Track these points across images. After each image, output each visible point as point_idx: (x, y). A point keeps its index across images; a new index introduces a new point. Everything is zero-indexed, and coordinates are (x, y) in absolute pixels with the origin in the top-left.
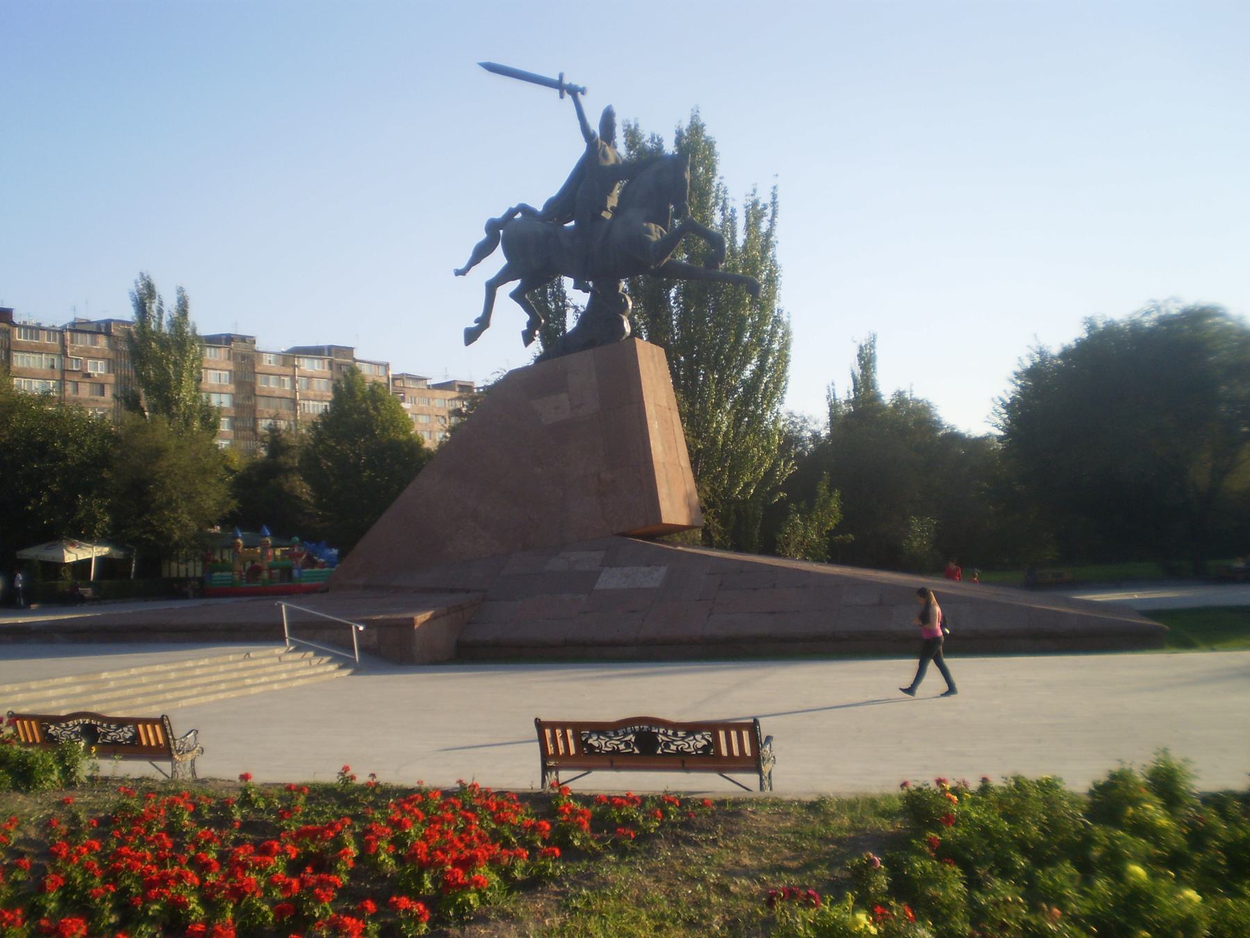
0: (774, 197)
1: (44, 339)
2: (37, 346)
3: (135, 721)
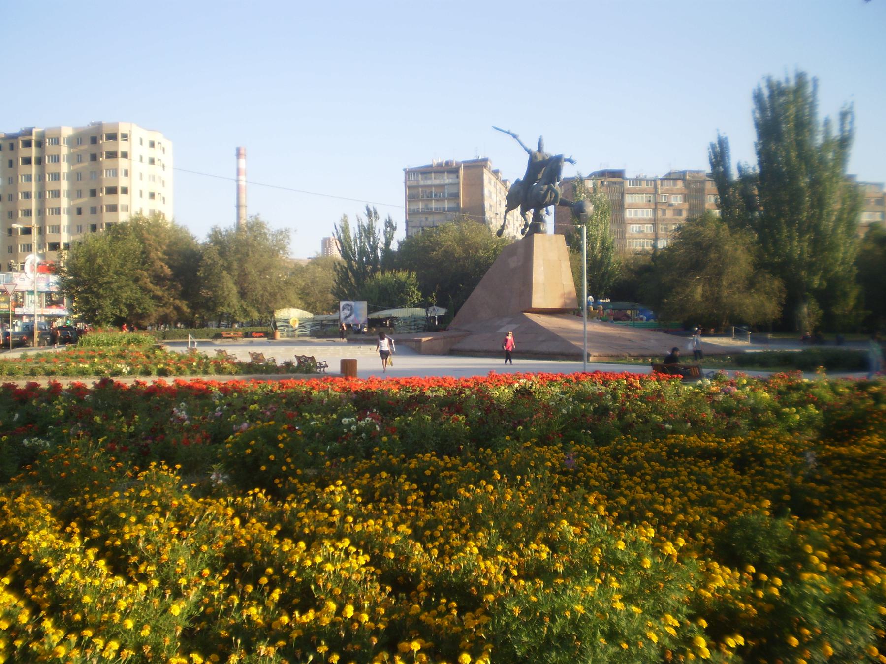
1: (644, 185)
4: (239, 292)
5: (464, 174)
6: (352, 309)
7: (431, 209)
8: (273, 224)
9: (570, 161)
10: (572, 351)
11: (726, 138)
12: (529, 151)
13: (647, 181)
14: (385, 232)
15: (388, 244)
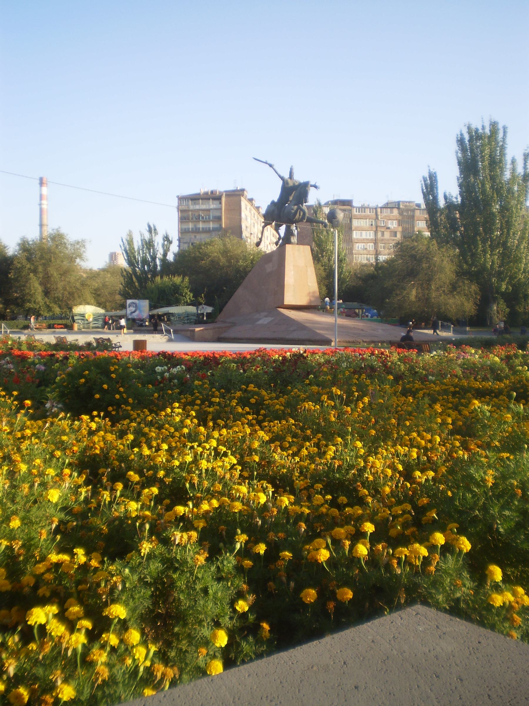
2: (364, 216)
4: (43, 291)
5: (226, 201)
6: (136, 306)
7: (199, 228)
8: (72, 235)
9: (315, 187)
10: (317, 338)
11: (435, 173)
12: (282, 178)
13: (370, 209)
14: (163, 245)
15: (165, 255)
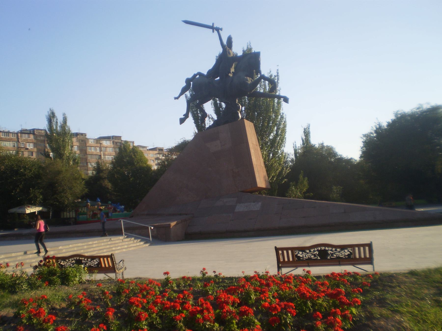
0: (278, 73)
1: (11, 136)
3: (99, 257)
